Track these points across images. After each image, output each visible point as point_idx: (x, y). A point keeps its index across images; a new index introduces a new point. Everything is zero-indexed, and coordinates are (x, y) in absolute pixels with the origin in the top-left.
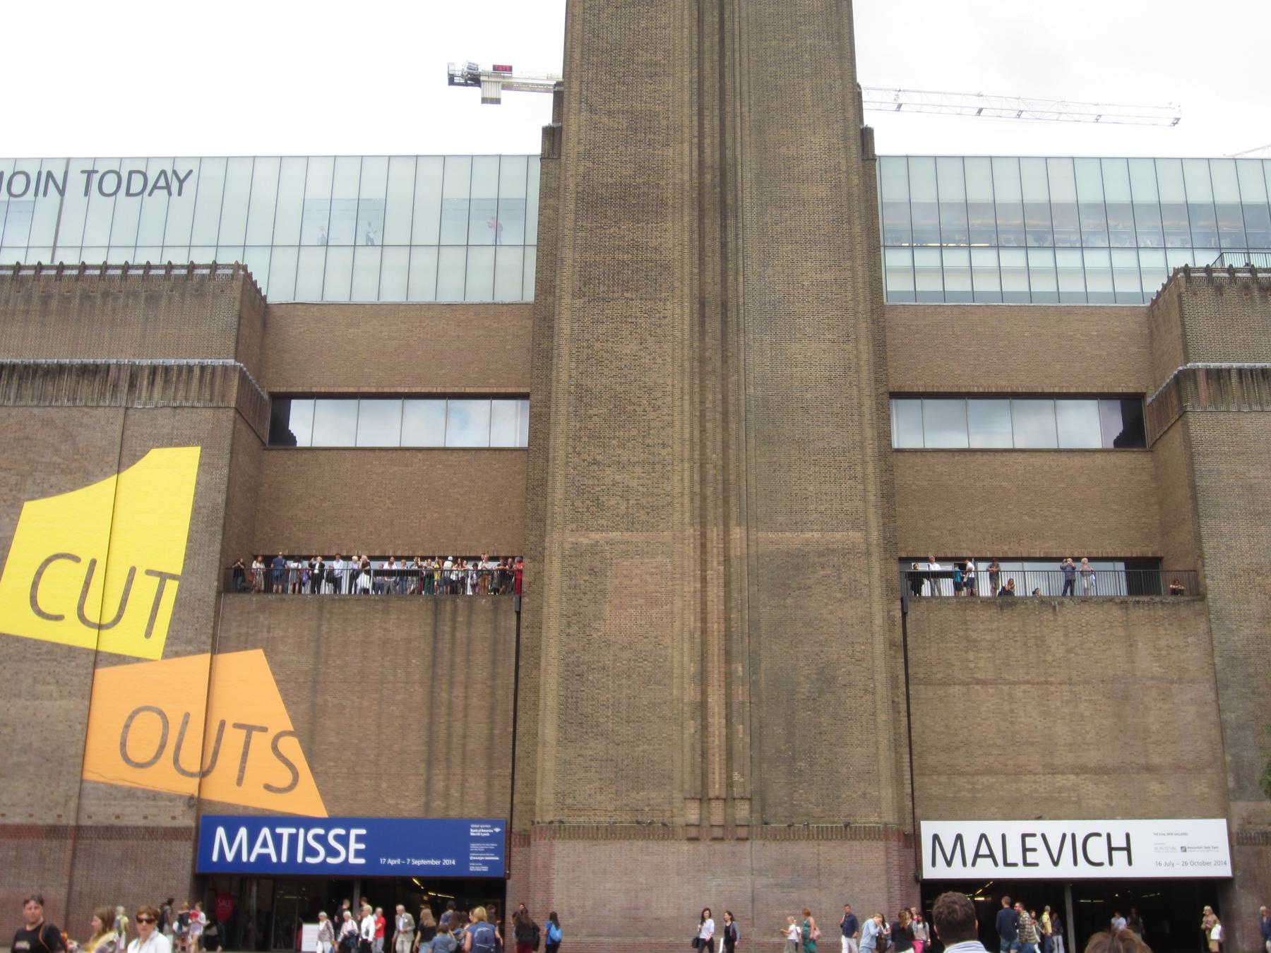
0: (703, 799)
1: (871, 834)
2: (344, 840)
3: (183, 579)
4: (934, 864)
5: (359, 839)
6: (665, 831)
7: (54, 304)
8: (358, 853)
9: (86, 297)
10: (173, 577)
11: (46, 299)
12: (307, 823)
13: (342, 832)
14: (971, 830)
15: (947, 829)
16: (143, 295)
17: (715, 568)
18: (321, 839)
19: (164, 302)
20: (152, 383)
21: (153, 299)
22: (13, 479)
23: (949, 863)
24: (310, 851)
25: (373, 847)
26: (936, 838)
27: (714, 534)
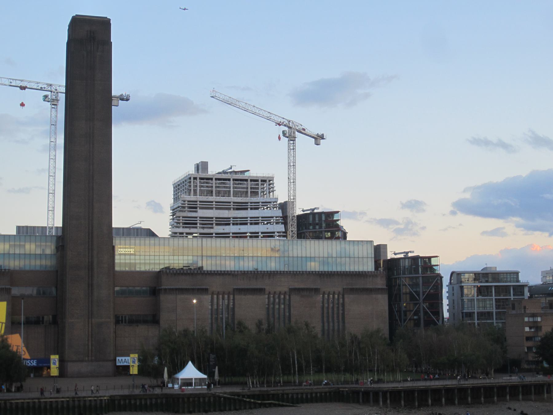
0: (88, 357)
1: (110, 361)
2: (33, 362)
3: (6, 323)
4: (118, 363)
5: (36, 362)
6: (82, 361)
8: (35, 364)
10: (4, 323)
12: (28, 360)
13: (33, 361)
14: (123, 358)
15: (120, 358)
17: (90, 325)
18: (30, 362)
23: (120, 363)
24: (28, 364)
25: (38, 363)
26: (119, 360)
27: (90, 320)
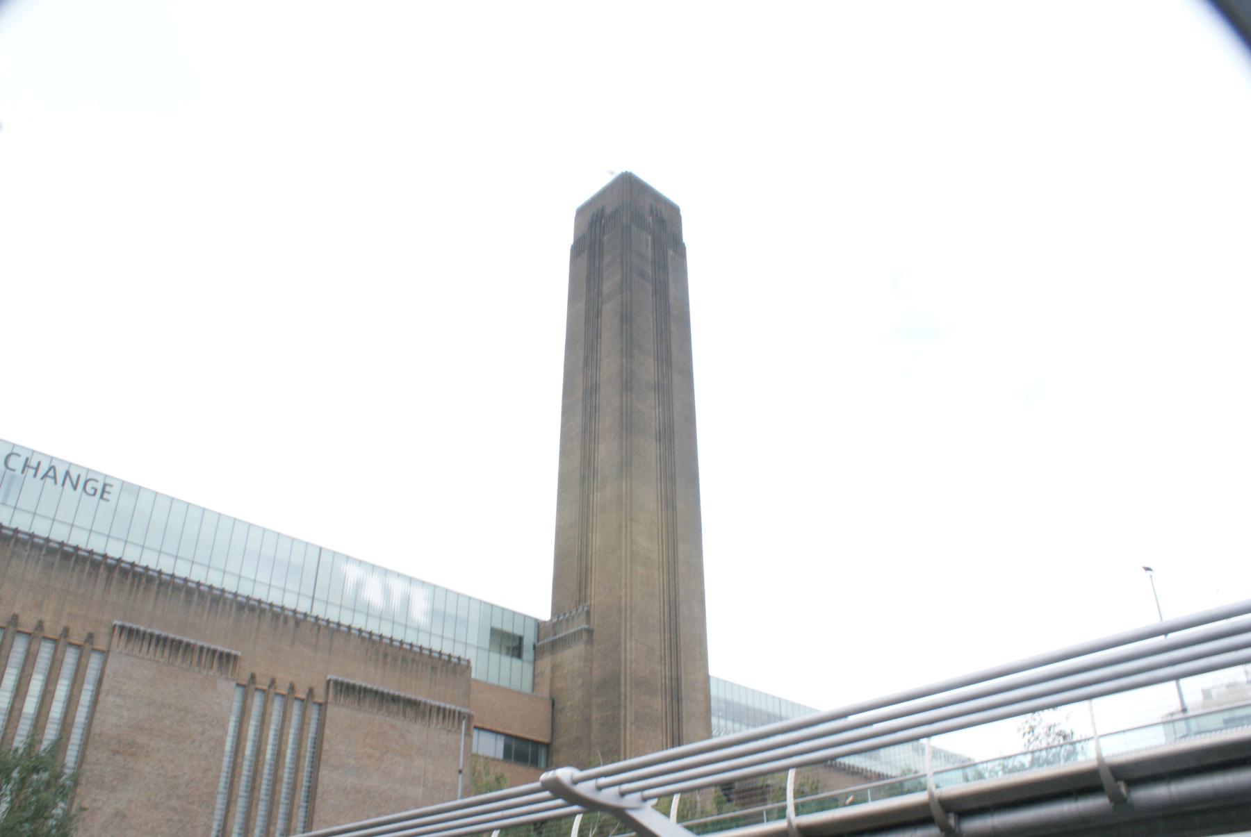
7: (389, 660)
9: (404, 660)
11: (386, 656)
16: (430, 666)
19: (439, 672)
20: (438, 714)
21: (434, 669)
22: (378, 755)
